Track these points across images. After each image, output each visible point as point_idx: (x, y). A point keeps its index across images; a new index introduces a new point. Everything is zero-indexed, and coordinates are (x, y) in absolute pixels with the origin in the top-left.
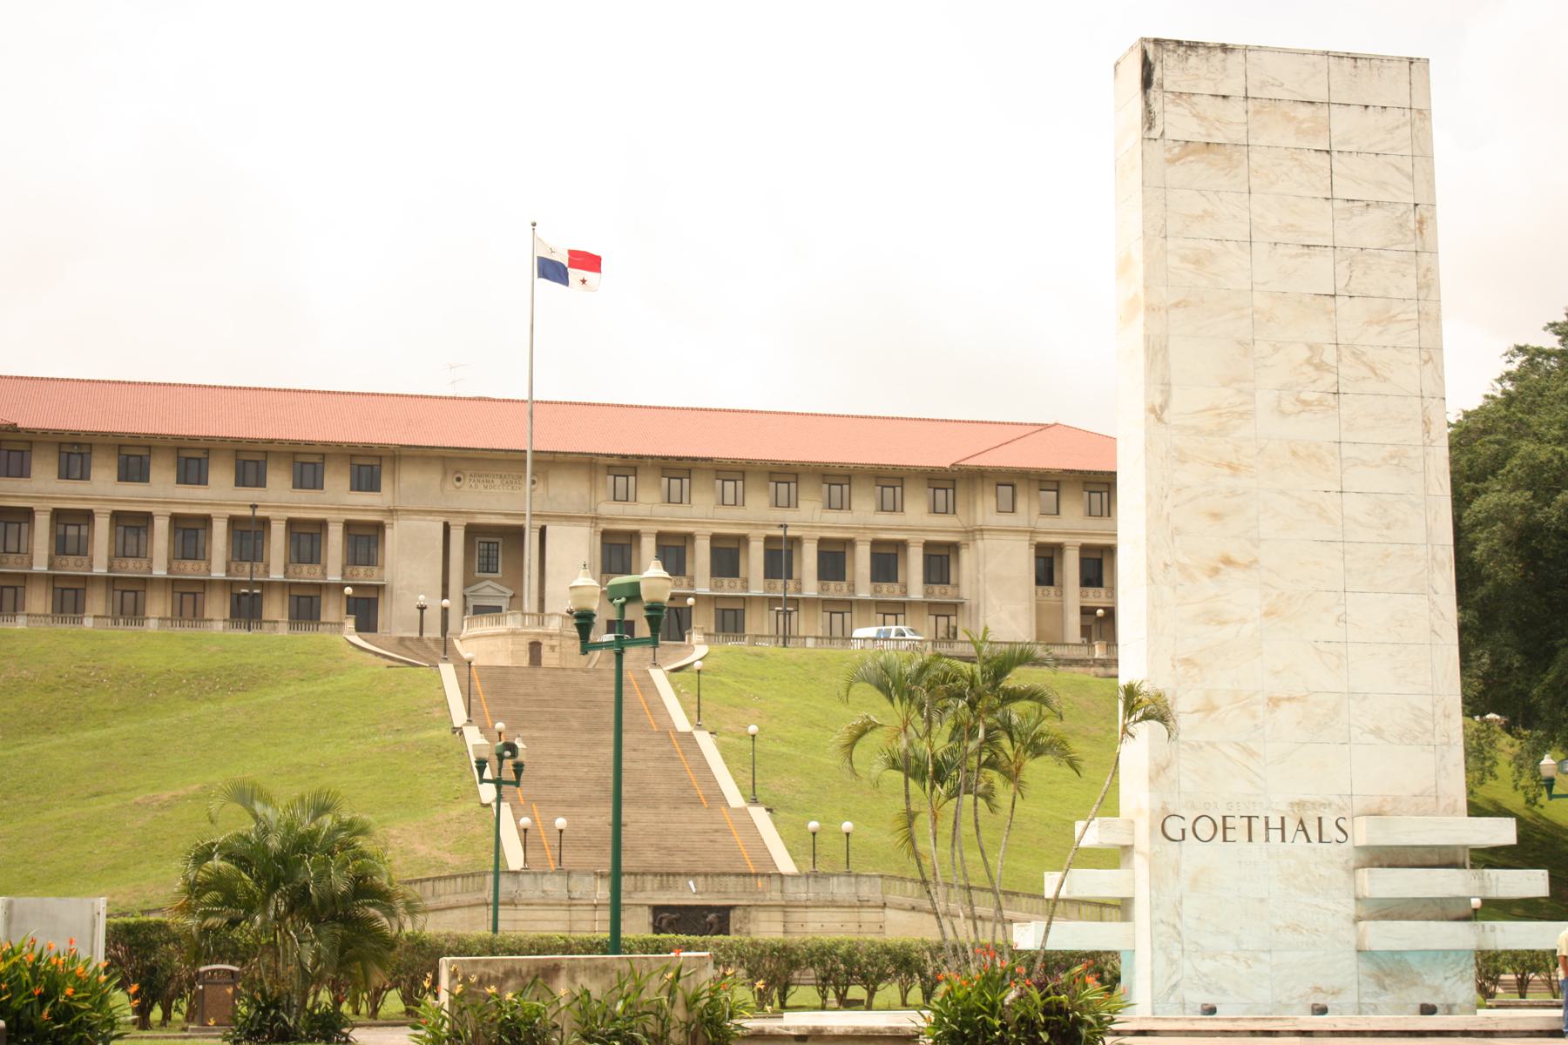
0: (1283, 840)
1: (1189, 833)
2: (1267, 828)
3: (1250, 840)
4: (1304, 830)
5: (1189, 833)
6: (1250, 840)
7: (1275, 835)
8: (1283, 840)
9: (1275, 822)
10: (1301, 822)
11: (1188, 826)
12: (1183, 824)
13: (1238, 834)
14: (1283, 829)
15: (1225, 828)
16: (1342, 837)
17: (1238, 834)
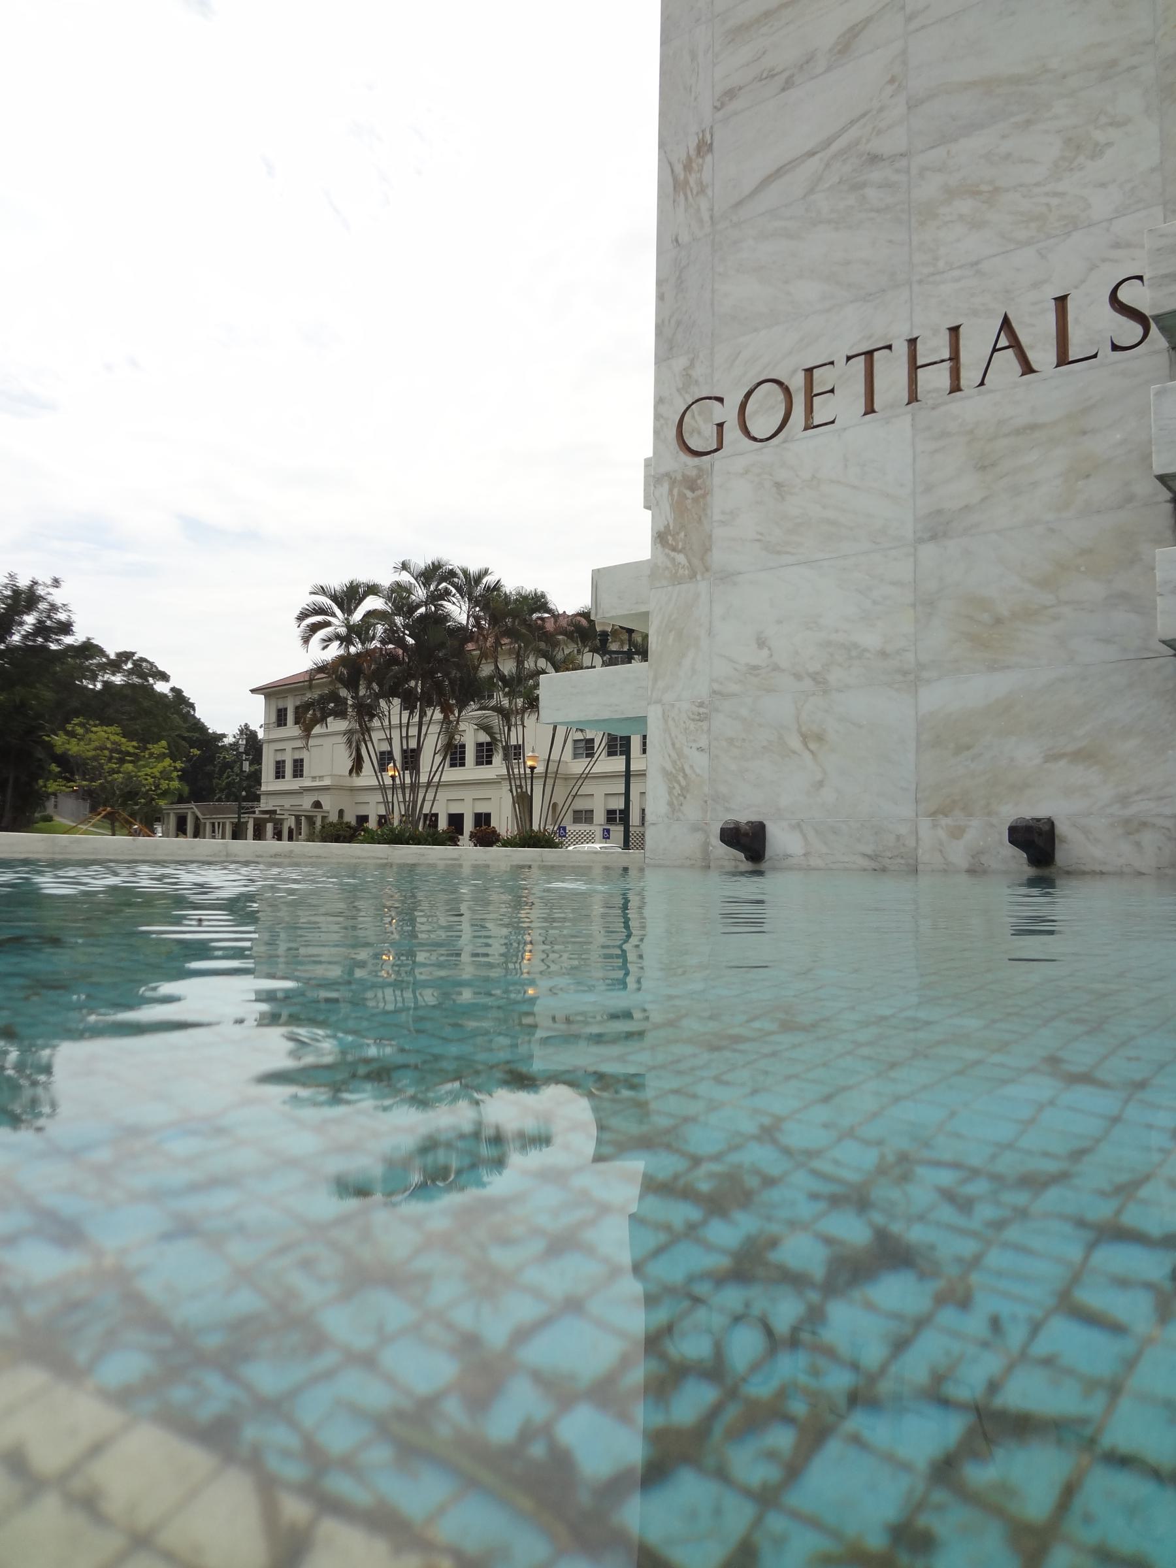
0: (956, 388)
1: (732, 433)
2: (914, 367)
3: (870, 409)
4: (1015, 344)
5: (732, 433)
6: (870, 409)
7: (935, 379)
8: (956, 388)
9: (935, 347)
10: (1006, 323)
11: (728, 413)
12: (719, 413)
13: (844, 405)
14: (955, 357)
15: (810, 396)
16: (1131, 331)
17: (844, 405)
